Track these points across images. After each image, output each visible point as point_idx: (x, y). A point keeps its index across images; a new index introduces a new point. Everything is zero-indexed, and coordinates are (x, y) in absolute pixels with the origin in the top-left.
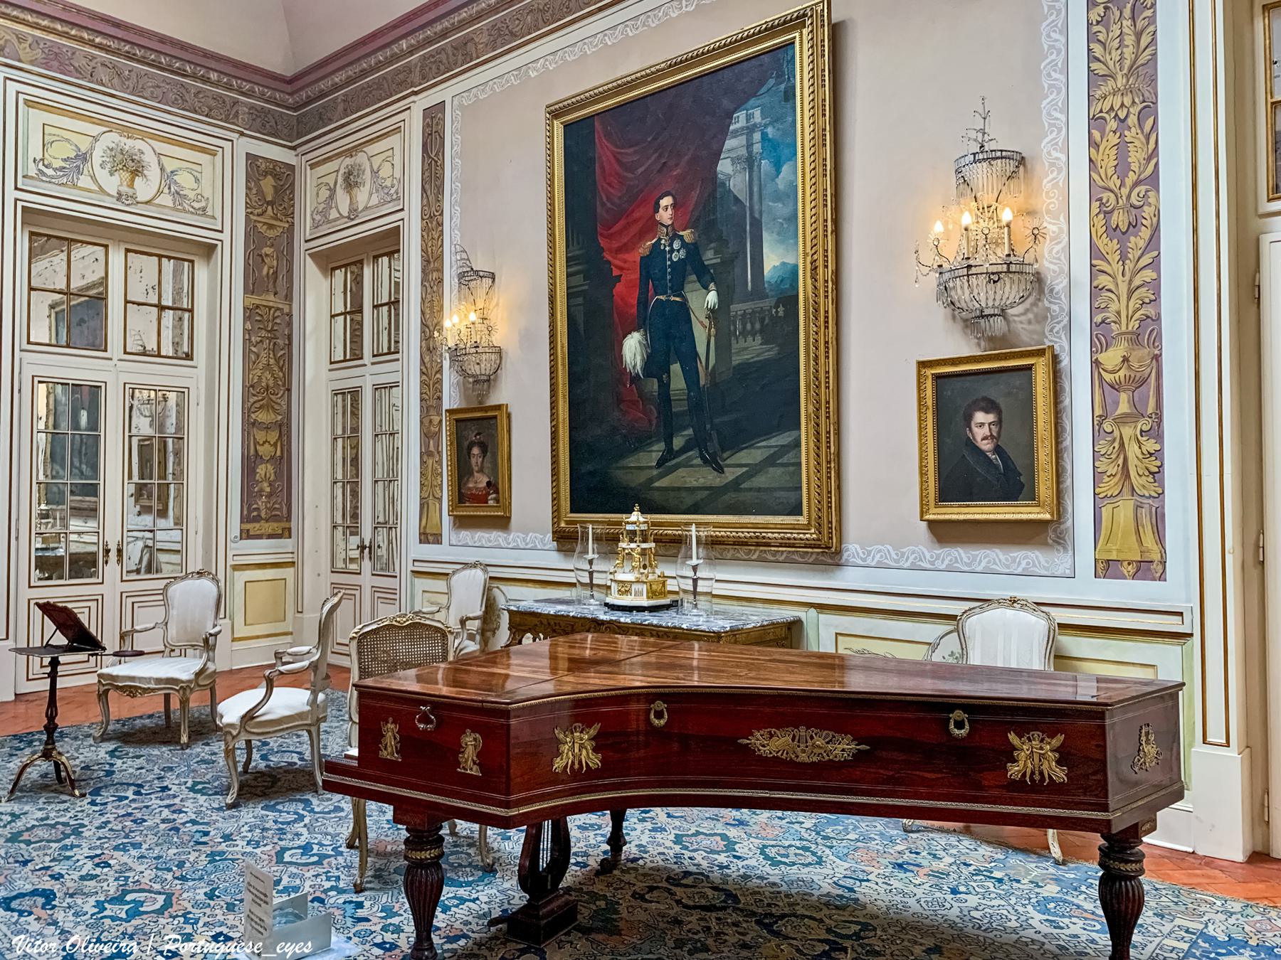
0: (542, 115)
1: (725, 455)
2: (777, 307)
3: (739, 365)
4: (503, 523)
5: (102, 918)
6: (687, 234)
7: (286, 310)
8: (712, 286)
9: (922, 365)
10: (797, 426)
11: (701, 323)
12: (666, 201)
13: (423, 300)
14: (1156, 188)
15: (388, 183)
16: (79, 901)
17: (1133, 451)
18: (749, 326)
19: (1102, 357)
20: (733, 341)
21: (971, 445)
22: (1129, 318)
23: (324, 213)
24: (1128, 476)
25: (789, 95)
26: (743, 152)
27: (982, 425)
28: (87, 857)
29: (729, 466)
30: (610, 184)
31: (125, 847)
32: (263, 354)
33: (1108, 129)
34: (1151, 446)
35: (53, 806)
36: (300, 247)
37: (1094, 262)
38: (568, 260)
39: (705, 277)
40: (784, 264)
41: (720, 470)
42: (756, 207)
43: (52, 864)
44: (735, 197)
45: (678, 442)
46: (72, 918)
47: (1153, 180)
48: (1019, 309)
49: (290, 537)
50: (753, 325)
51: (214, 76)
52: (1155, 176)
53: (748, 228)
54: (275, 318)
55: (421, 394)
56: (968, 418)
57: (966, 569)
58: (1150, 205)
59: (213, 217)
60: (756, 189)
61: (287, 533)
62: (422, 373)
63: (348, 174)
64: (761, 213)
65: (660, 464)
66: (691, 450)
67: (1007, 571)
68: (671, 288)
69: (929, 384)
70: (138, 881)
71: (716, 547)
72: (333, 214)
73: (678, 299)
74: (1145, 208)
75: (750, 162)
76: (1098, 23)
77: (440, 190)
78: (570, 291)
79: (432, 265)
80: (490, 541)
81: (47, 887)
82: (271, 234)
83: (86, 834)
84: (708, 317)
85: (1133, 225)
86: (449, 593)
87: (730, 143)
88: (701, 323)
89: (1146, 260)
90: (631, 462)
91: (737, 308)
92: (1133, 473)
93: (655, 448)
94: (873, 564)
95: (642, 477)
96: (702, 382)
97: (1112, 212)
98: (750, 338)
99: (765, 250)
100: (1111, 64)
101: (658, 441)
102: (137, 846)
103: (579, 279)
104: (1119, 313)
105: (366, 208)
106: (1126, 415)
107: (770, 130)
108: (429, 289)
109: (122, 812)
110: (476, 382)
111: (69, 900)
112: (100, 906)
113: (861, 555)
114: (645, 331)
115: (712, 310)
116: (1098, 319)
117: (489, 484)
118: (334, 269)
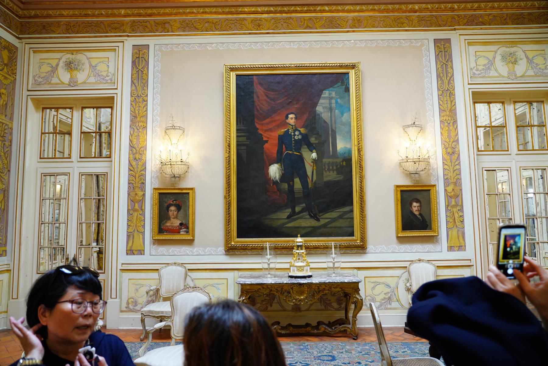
1: (321, 214)
2: (343, 162)
3: (327, 181)
4: (190, 242)
6: (302, 130)
7: (10, 126)
8: (314, 151)
9: (397, 186)
10: (351, 204)
11: (310, 164)
12: (291, 116)
14: (458, 143)
15: (104, 74)
17: (456, 215)
18: (331, 168)
19: (447, 188)
20: (324, 172)
21: (412, 213)
22: (454, 178)
24: (455, 222)
25: (347, 90)
26: (328, 105)
27: (415, 207)
30: (262, 104)
33: (445, 125)
34: (461, 214)
37: (444, 161)
38: (237, 130)
39: (311, 147)
41: (318, 220)
42: (334, 126)
44: (324, 120)
45: (297, 209)
47: (457, 141)
48: (421, 173)
49: (6, 255)
50: (333, 168)
52: (458, 140)
53: (330, 132)
54: (5, 129)
55: (129, 180)
57: (410, 251)
58: (457, 148)
60: (333, 119)
64: (336, 128)
65: (289, 217)
67: (422, 251)
69: (399, 193)
71: (311, 250)
72: (55, 80)
74: (456, 149)
75: (331, 109)
76: (441, 95)
78: (238, 143)
79: (138, 119)
80: (181, 252)
84: (313, 162)
85: (453, 153)
86: (160, 279)
87: (321, 101)
88: (310, 164)
89: (457, 163)
90: (274, 216)
91: (325, 160)
92: (456, 221)
93: (287, 211)
94: (378, 252)
95: (279, 223)
96: (310, 186)
97: (447, 148)
98: (331, 172)
100: (445, 107)
101: (288, 208)
103: (243, 139)
104: (451, 176)
105: (84, 83)
106: (454, 205)
107: (339, 100)
108: (136, 130)
113: (374, 249)
115: (314, 160)
116: (445, 178)
117: (181, 224)
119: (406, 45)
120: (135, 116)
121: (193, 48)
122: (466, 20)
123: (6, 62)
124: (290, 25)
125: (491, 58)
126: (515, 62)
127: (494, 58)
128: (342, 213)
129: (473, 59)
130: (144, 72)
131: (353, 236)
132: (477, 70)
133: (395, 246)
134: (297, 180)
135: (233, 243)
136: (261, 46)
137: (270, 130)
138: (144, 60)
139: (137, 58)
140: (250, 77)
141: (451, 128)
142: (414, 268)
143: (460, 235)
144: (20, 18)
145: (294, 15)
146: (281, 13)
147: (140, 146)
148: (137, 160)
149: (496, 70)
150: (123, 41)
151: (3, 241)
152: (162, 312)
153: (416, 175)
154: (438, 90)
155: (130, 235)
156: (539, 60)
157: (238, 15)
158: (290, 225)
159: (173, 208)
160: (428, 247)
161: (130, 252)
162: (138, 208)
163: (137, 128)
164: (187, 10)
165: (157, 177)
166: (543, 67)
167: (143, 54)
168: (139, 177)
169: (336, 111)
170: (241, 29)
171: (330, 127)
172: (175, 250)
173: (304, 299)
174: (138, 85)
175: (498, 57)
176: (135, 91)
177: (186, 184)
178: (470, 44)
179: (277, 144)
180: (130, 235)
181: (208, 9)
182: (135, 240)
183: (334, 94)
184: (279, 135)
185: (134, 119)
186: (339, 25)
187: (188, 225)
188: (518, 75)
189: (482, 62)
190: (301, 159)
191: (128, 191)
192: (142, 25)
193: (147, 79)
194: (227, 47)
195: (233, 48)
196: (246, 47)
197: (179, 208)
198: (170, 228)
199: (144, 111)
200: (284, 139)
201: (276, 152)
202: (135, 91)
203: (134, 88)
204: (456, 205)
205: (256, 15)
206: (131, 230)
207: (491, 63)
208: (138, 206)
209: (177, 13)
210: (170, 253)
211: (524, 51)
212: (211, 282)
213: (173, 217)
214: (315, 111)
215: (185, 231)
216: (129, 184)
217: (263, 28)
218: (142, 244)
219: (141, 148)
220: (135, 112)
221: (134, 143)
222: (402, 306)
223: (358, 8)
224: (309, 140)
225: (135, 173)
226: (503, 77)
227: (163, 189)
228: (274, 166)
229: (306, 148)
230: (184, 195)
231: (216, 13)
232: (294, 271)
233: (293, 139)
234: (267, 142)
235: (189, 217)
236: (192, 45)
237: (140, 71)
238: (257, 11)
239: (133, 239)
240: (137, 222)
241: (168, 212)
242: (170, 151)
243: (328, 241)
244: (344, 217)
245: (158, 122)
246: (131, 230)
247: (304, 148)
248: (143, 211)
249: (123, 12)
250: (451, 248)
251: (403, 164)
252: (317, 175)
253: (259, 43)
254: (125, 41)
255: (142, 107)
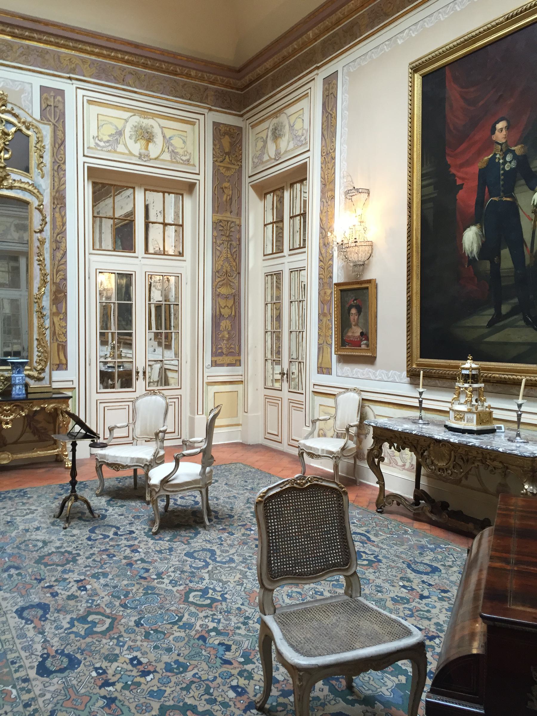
0: (406, 71)
5: (70, 633)
7: (237, 223)
11: (528, 217)
13: (321, 212)
15: (300, 133)
16: (61, 617)
23: (260, 157)
28: (75, 581)
31: (99, 575)
32: (224, 251)
35: (68, 537)
36: (246, 182)
38: (423, 176)
43: (55, 584)
46: (53, 630)
51: (193, 73)
54: (231, 228)
59: (194, 165)
63: (275, 130)
68: (503, 191)
70: (99, 605)
72: (266, 158)
73: (508, 199)
78: (424, 198)
79: (327, 187)
81: (47, 602)
82: (228, 173)
83: (80, 562)
88: (528, 217)
102: (105, 575)
103: (431, 189)
105: (286, 152)
108: (325, 203)
109: (103, 547)
110: (355, 266)
111: (56, 615)
112: (72, 623)
118: (266, 194)
123: (227, 150)
134: (505, 252)
137: (468, 163)
144: (242, 90)
151: (235, 350)
179: (477, 189)
216: (319, 279)
224: (529, 167)
228: (470, 230)
229: (523, 185)
234: (461, 187)
247: (520, 186)
249: (310, 34)
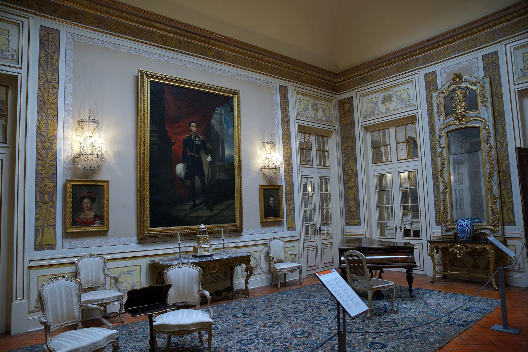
1: (214, 206)
4: (104, 234)
8: (209, 154)
9: (262, 186)
10: (234, 198)
11: (206, 165)
12: (193, 124)
17: (291, 206)
18: (221, 169)
19: (286, 188)
21: (269, 205)
25: (232, 110)
26: (219, 120)
27: (271, 200)
29: (214, 209)
34: (293, 206)
38: (150, 130)
39: (208, 152)
40: (230, 154)
41: (212, 211)
42: (223, 136)
45: (198, 202)
53: (220, 141)
55: (37, 170)
56: (269, 199)
60: (222, 131)
61: (359, 224)
62: (38, 159)
65: (191, 208)
66: (203, 204)
73: (198, 156)
75: (221, 123)
77: (56, 70)
84: (208, 164)
85: (289, 164)
87: (215, 116)
88: (206, 165)
89: (291, 171)
91: (217, 163)
92: (291, 210)
93: (190, 203)
96: (206, 183)
99: (225, 149)
106: (290, 200)
107: (226, 117)
108: (44, 117)
114: (185, 164)
115: (210, 162)
117: (95, 216)
119: (264, 84)
120: (44, 101)
121: (107, 46)
122: (295, 77)
124: (189, 49)
125: (306, 104)
126: (317, 110)
127: (308, 105)
128: (227, 205)
129: (298, 103)
130: (55, 58)
131: (235, 223)
132: (300, 111)
133: (259, 229)
134: (197, 178)
135: (146, 233)
136: (167, 60)
138: (54, 45)
139: (45, 40)
140: (162, 85)
141: (288, 147)
142: (273, 243)
143: (293, 220)
145: (192, 41)
146: (184, 36)
147: (50, 134)
148: (46, 150)
149: (309, 113)
150: (29, 17)
152: (103, 299)
153: (271, 178)
154: (282, 120)
155: (39, 229)
156: (327, 111)
157: (150, 28)
158: (192, 215)
159: (86, 200)
160: (277, 228)
161: (39, 247)
162: (48, 200)
163: (46, 115)
164: (104, 8)
165: (70, 168)
166: (328, 116)
167: (53, 38)
168: (49, 167)
169: (225, 125)
170: (151, 41)
171: (220, 137)
172: (90, 242)
173: (216, 273)
174: (48, 70)
175: (310, 105)
176: (43, 75)
177: (102, 176)
178: (297, 93)
180: (39, 229)
181: (124, 14)
182: (44, 234)
183: (223, 112)
184: (184, 139)
185: (42, 105)
186: (224, 58)
187: (102, 217)
188: (319, 119)
189: (303, 106)
190: (200, 160)
191: (36, 182)
192: (52, 7)
193: (57, 65)
194: (139, 53)
195: (144, 56)
196: (155, 57)
197: (93, 200)
198: (84, 220)
199: (54, 98)
200: (188, 143)
201: (181, 153)
202: (43, 75)
203: (42, 72)
204: (290, 200)
205: (164, 32)
206: (39, 223)
207: (306, 108)
208: (49, 198)
209: (93, 8)
210: (85, 245)
211: (321, 104)
212: (125, 270)
213: (87, 209)
214: (211, 123)
215: (99, 223)
216: (37, 174)
217: (169, 45)
218: (54, 238)
219: (51, 136)
220: (44, 98)
221: (43, 130)
222: (263, 271)
223: (238, 49)
225: (45, 163)
226: (312, 118)
227: (77, 181)
230: (99, 188)
231: (130, 20)
232: (201, 251)
233: (194, 144)
234: (174, 143)
235: (103, 208)
236: (106, 43)
237: (49, 55)
238: (166, 29)
239: (43, 233)
240: (47, 215)
241: (82, 204)
242: (92, 143)
243: (218, 227)
244: (229, 208)
245: (70, 112)
246: (39, 223)
248: (54, 203)
250: (288, 229)
251: (263, 170)
252: (211, 174)
253: (166, 57)
254: (31, 18)
255: (53, 92)
